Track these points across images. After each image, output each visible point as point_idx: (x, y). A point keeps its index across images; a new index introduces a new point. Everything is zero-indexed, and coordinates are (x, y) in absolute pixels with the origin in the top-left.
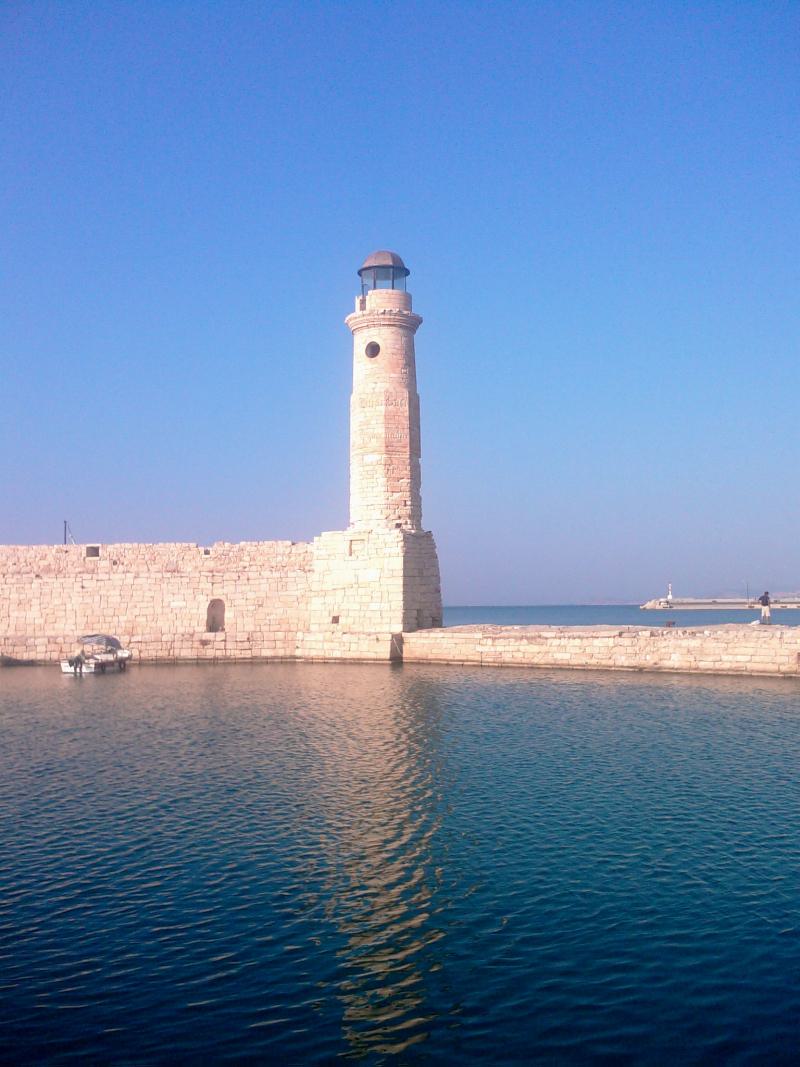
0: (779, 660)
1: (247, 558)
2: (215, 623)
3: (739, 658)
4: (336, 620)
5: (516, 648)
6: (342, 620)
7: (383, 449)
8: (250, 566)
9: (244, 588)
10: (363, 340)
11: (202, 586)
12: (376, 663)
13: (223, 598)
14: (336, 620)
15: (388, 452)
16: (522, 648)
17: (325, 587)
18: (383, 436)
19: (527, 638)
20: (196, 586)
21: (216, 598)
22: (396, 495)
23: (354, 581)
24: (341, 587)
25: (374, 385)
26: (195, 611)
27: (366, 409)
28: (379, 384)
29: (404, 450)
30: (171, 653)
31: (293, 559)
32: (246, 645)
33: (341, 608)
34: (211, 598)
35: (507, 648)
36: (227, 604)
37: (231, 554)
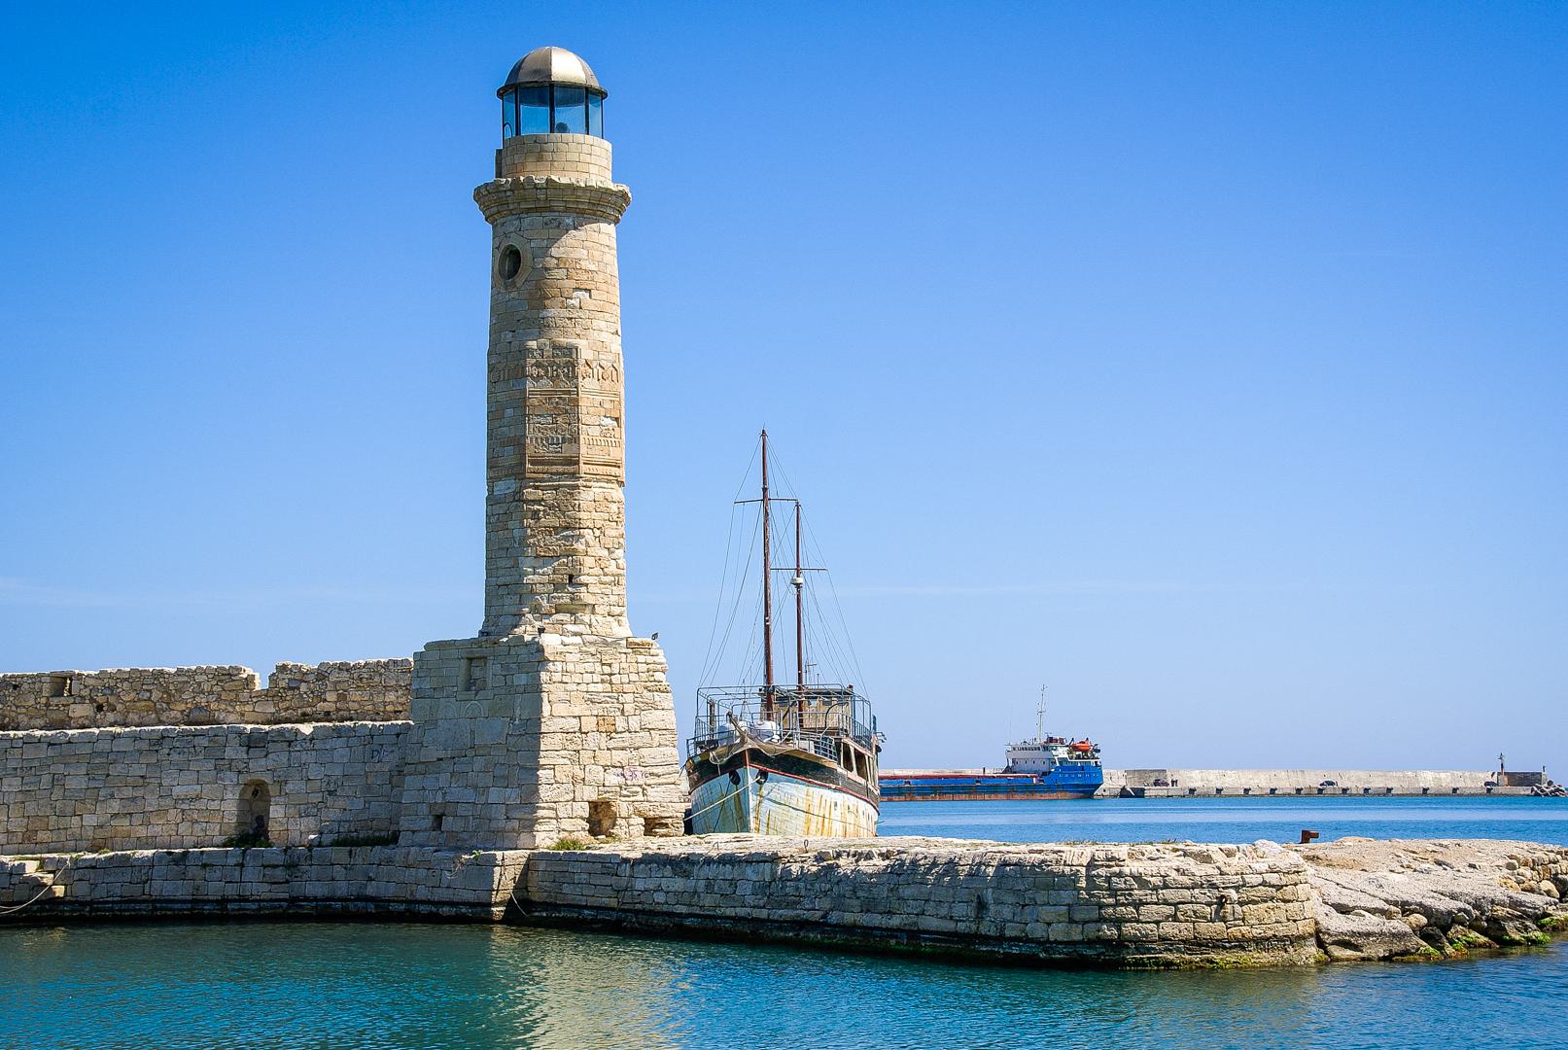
1: (331, 697)
2: (252, 833)
6: (448, 823)
9: (304, 757)
11: (229, 753)
13: (267, 779)
20: (219, 754)
21: (255, 777)
26: (215, 805)
30: (147, 891)
33: (448, 798)
34: (245, 778)
36: (273, 790)
37: (303, 687)
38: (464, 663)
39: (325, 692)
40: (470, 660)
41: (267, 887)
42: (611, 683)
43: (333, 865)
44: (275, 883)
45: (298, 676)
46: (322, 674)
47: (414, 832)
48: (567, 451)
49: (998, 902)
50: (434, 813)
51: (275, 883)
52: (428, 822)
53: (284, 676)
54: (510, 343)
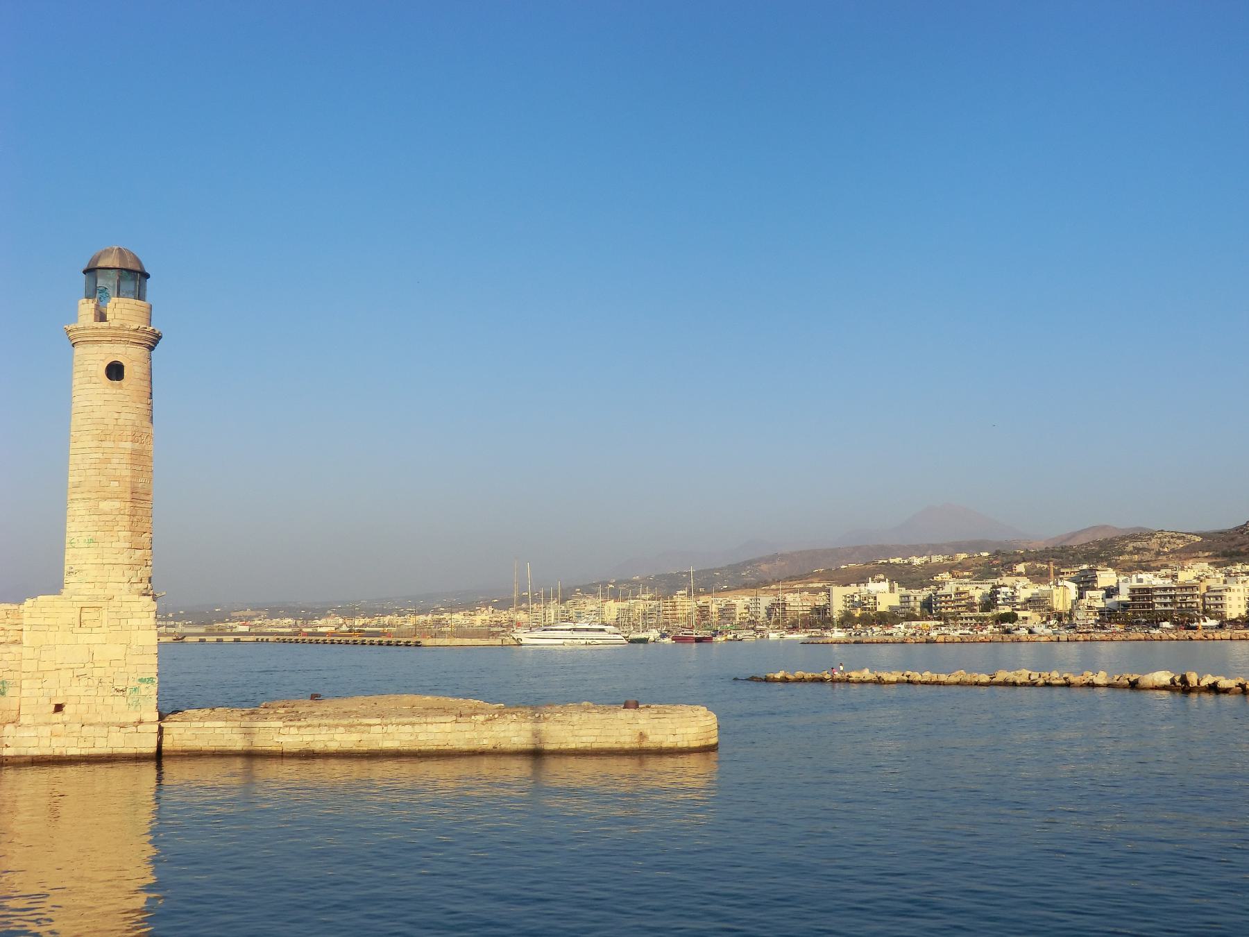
0: (622, 740)
3: (584, 739)
4: (59, 708)
7: (128, 496)
12: (138, 758)
14: (59, 708)
15: (133, 500)
16: (337, 737)
18: (128, 479)
19: (343, 726)
22: (139, 553)
25: (116, 416)
27: (104, 444)
28: (123, 416)
33: (68, 693)
35: (318, 738)
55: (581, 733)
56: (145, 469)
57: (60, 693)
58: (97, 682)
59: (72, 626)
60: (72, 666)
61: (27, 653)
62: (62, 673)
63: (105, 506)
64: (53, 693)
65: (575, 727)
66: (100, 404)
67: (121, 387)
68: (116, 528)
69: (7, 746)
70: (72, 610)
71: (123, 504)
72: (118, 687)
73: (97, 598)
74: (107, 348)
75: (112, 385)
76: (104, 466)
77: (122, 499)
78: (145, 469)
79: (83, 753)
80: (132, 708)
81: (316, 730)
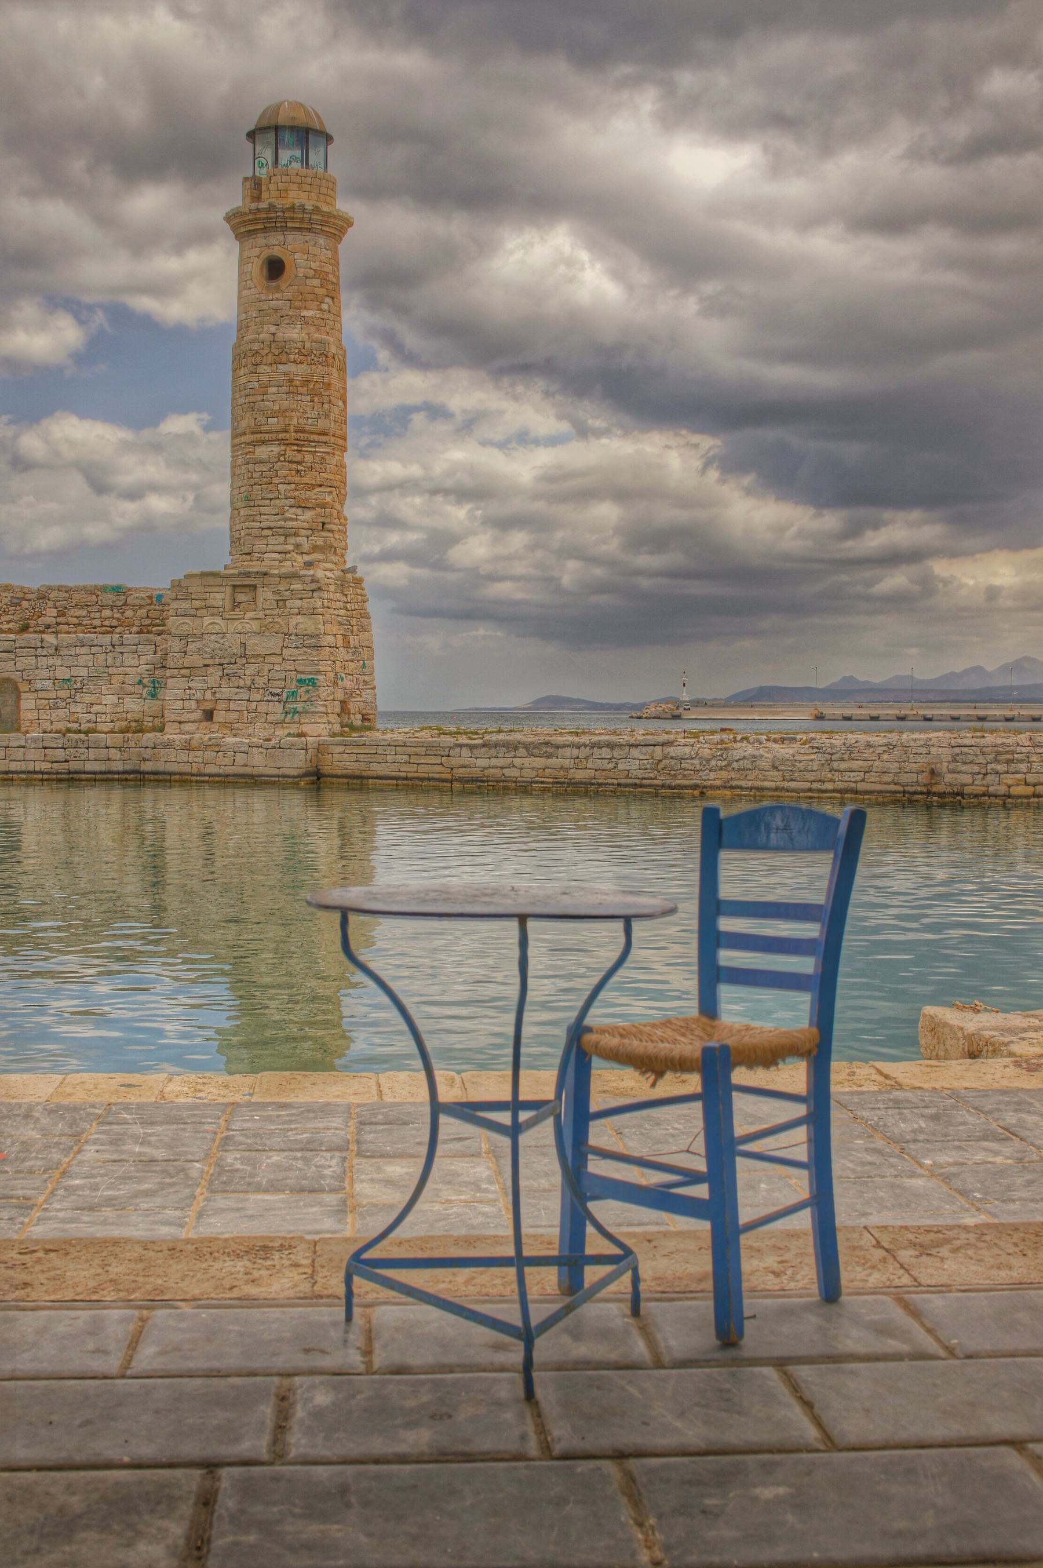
0: (905, 778)
1: (53, 612)
4: (209, 715)
5: (509, 760)
6: (219, 716)
8: (58, 624)
9: (51, 661)
10: (257, 251)
13: (16, 676)
16: (517, 762)
17: (188, 661)
22: (308, 515)
23: (238, 650)
24: (217, 661)
25: (273, 329)
29: (323, 438)
31: (129, 613)
32: (60, 754)
33: (218, 696)
35: (494, 762)
36: (23, 687)
37: (25, 604)
38: (229, 589)
39: (45, 609)
40: (234, 587)
41: (49, 765)
42: (347, 610)
43: (108, 748)
44: (56, 762)
45: (20, 595)
46: (43, 596)
47: (180, 723)
48: (322, 424)
49: (950, 772)
50: (203, 708)
51: (56, 762)
52: (198, 715)
53: (6, 595)
54: (274, 334)
55: (843, 766)
56: (316, 399)
57: (208, 695)
58: (249, 683)
59: (221, 610)
60: (222, 661)
61: (174, 644)
62: (211, 670)
63: (262, 452)
64: (199, 696)
65: (834, 757)
66: (254, 315)
67: (278, 289)
68: (276, 480)
69: (144, 760)
70: (222, 589)
71: (283, 448)
72: (273, 690)
73: (248, 575)
74: (260, 240)
75: (268, 289)
76: (259, 398)
77: (282, 442)
78: (316, 399)
79: (221, 771)
80: (289, 716)
81: (493, 752)
